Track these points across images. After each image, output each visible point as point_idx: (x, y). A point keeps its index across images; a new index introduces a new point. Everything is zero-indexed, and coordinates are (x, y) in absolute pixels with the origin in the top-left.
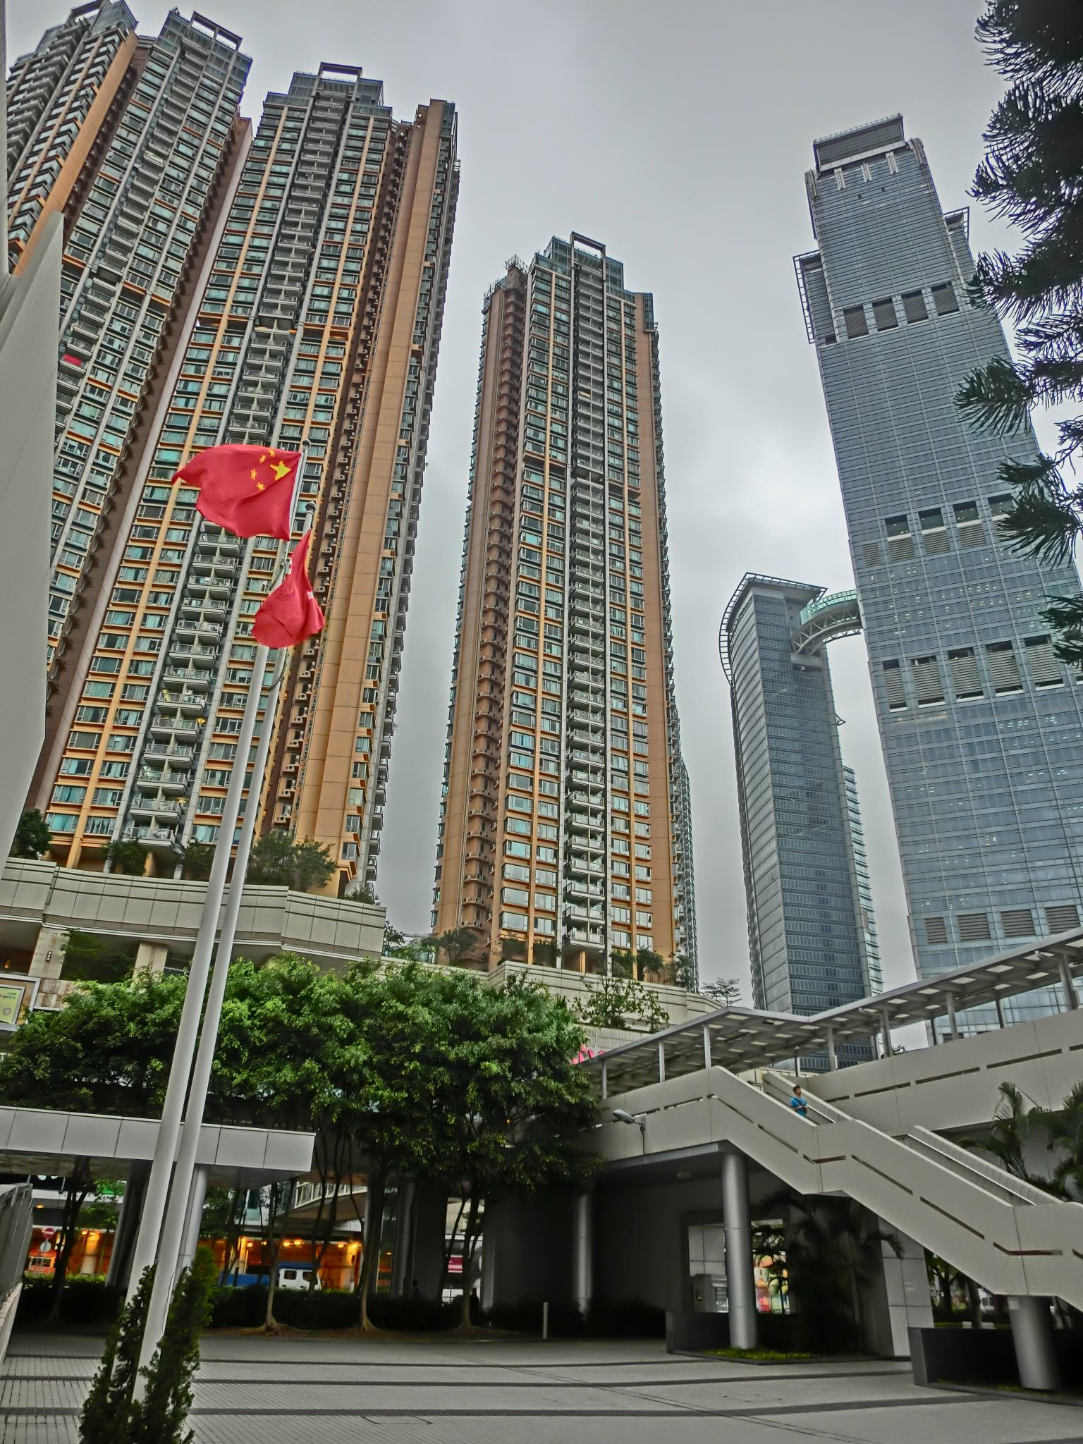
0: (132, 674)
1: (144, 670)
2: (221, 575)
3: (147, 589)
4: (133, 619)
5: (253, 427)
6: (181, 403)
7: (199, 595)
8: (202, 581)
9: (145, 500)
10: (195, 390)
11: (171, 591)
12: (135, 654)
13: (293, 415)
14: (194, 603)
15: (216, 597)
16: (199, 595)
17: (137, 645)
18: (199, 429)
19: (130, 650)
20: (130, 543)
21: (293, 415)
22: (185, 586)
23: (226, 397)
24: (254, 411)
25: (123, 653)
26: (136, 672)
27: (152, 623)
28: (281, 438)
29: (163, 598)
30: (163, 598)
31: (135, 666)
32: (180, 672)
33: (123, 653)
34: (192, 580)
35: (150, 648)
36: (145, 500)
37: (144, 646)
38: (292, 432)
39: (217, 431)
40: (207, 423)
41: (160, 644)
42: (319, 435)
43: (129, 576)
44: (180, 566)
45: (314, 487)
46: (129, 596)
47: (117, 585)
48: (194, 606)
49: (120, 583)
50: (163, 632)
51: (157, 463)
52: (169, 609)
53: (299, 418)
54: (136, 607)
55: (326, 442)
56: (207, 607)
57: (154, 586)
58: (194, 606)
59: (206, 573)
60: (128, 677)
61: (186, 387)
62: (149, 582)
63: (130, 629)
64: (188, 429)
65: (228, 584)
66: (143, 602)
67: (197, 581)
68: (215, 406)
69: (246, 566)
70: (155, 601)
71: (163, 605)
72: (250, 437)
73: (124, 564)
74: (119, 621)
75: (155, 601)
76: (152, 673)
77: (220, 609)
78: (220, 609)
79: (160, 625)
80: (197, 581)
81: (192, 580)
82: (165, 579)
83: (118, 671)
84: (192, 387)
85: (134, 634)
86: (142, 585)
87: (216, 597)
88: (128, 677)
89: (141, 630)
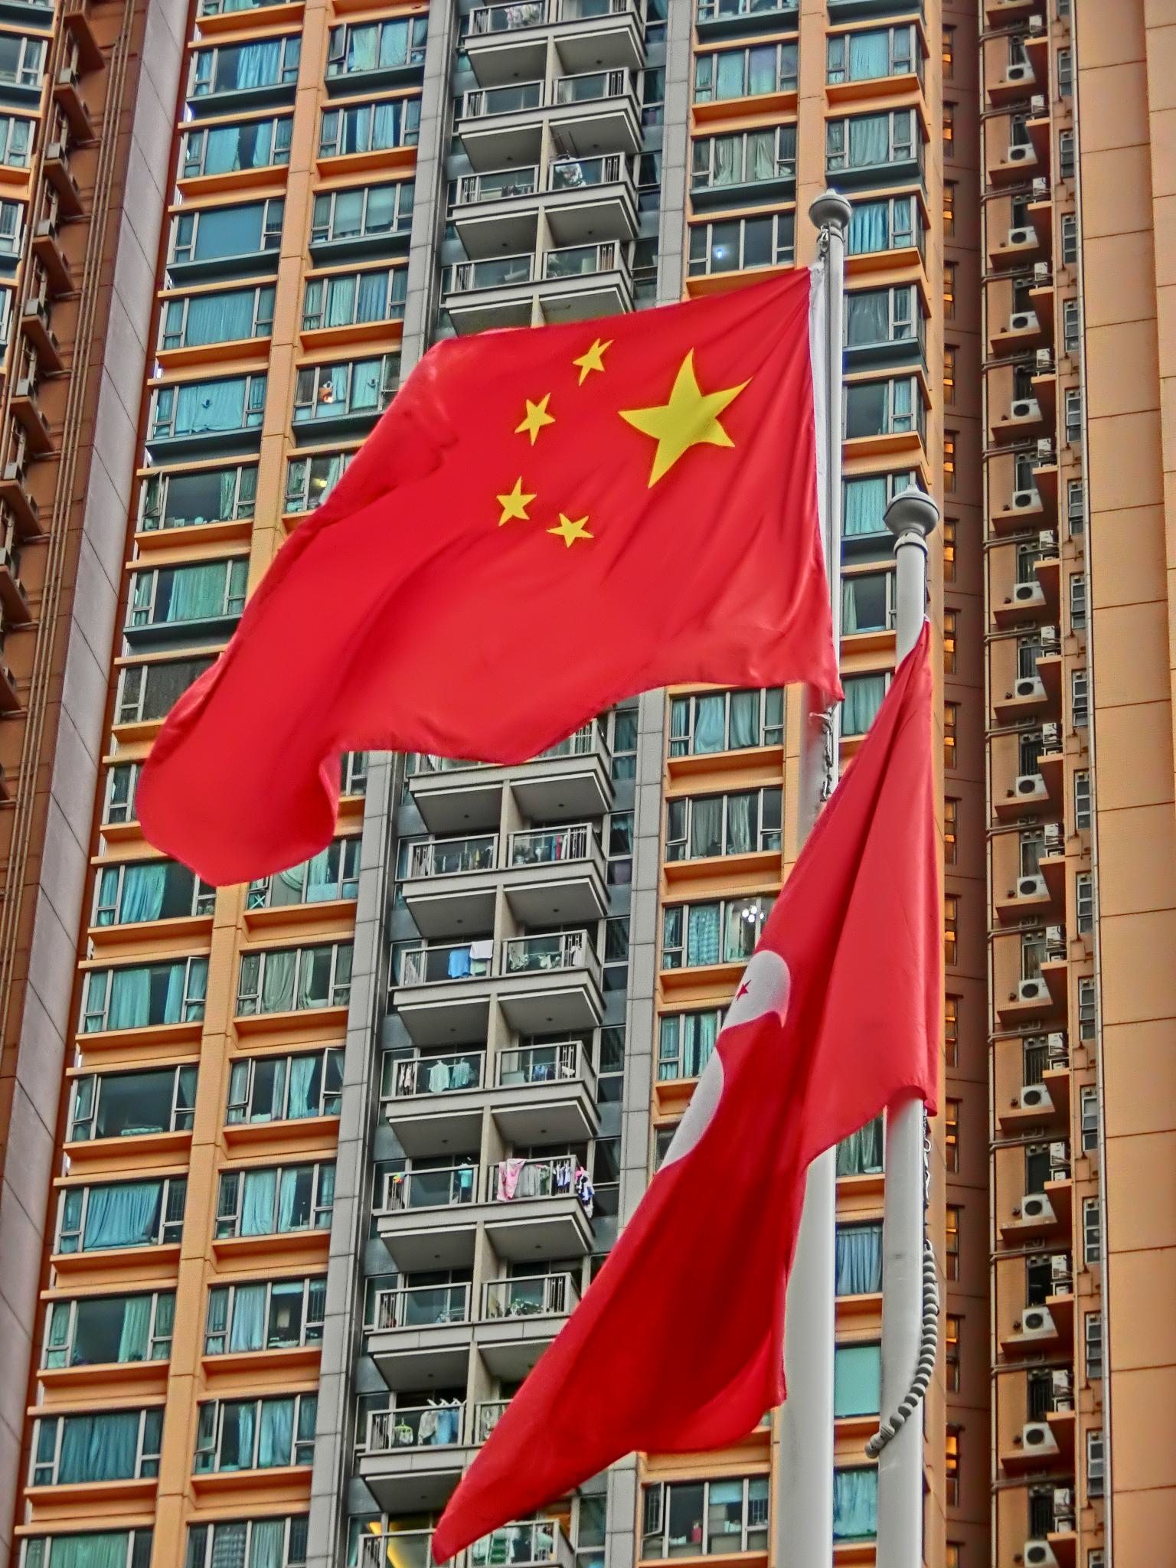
0: (218, 1473)
1: (264, 1439)
2: (541, 924)
3: (213, 1054)
4: (177, 1209)
5: (560, 180)
6: (220, 153)
7: (458, 1037)
8: (456, 964)
9: (139, 640)
10: (275, 81)
11: (324, 1041)
12: (212, 1371)
13: (730, 83)
14: (439, 1076)
15: (539, 1034)
16: (458, 1037)
17: (217, 1329)
18: (319, 257)
19: (185, 1359)
20: (72, 1173)
21: (730, 83)
22: (385, 1008)
23: (415, 76)
24: (556, 105)
25: (160, 1374)
26: (230, 1455)
27: (264, 1209)
28: (700, 203)
29: (297, 1078)
30: (297, 1078)
31: (223, 1430)
32: (432, 1418)
33: (160, 1374)
34: (411, 969)
35: (275, 1333)
36: (139, 640)
37: (249, 1328)
38: (744, 165)
39: (401, 246)
40: (351, 218)
41: (318, 1301)
42: (874, 146)
43: (127, 1006)
44: (346, 913)
45: (899, 401)
46: (142, 1103)
47: (81, 1064)
48: (443, 1093)
49: (92, 1048)
50: (321, 1244)
51: (162, 453)
52: (331, 1130)
53: (764, 88)
54: (184, 1146)
55: (913, 172)
56: (504, 1086)
57: (244, 1031)
58: (443, 1093)
59: (470, 923)
60: (201, 1490)
61: (227, 76)
62: (218, 1019)
63: (172, 1259)
64: (270, 264)
65: (581, 956)
66: (208, 1123)
67: (438, 971)
68: (376, 130)
69: (648, 856)
70: (262, 1104)
71: (300, 1114)
72: (558, 240)
73: (97, 957)
74: (115, 1227)
75: (262, 1104)
76: (306, 1452)
77: (567, 1084)
78: (567, 1084)
79: (301, 1212)
80: (438, 971)
81: (411, 969)
82: (285, 988)
83: (152, 1468)
84: (254, 73)
85: (192, 1279)
86: (193, 1036)
87: (539, 1034)
88: (201, 1490)
89: (222, 1254)
